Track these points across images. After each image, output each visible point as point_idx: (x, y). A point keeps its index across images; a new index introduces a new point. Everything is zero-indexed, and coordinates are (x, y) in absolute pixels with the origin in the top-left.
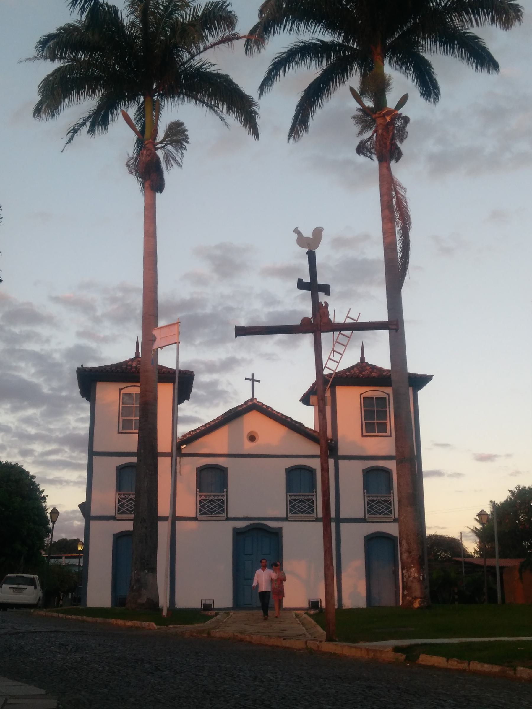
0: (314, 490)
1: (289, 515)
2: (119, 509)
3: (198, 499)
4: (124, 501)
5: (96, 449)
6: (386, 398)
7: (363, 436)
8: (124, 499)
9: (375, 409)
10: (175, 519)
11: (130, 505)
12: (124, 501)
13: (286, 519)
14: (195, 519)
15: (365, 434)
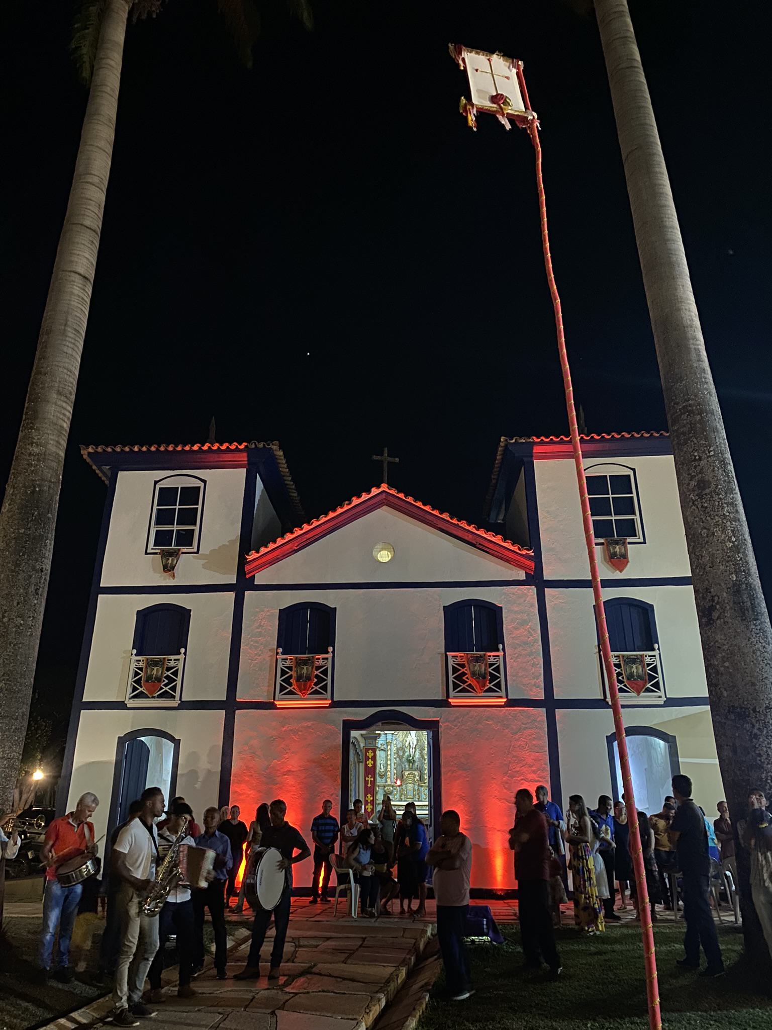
0: (501, 646)
1: (452, 693)
2: (135, 689)
3: (280, 666)
6: (629, 476)
9: (611, 496)
13: (444, 704)
14: (270, 706)
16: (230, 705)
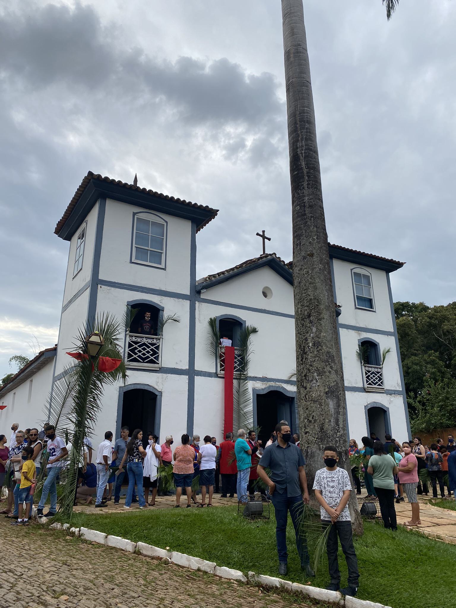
4: (135, 346)
5: (101, 277)
7: (356, 308)
8: (136, 343)
10: (191, 373)
11: (143, 352)
12: (135, 346)
15: (357, 307)
16: (191, 373)
